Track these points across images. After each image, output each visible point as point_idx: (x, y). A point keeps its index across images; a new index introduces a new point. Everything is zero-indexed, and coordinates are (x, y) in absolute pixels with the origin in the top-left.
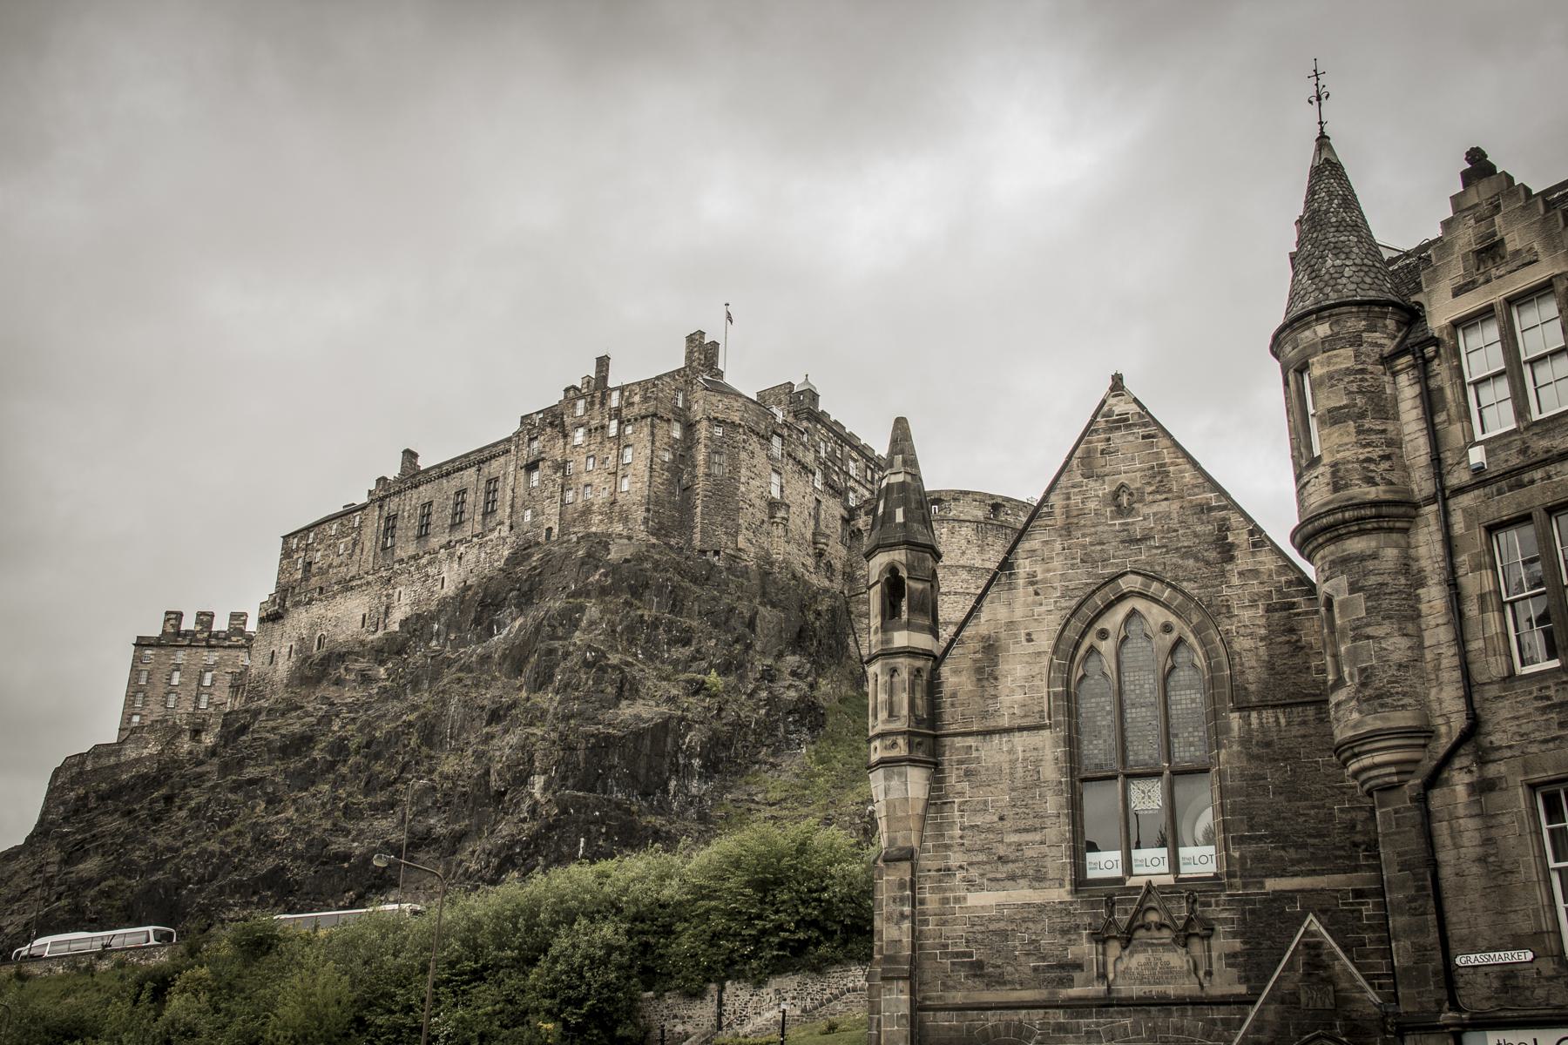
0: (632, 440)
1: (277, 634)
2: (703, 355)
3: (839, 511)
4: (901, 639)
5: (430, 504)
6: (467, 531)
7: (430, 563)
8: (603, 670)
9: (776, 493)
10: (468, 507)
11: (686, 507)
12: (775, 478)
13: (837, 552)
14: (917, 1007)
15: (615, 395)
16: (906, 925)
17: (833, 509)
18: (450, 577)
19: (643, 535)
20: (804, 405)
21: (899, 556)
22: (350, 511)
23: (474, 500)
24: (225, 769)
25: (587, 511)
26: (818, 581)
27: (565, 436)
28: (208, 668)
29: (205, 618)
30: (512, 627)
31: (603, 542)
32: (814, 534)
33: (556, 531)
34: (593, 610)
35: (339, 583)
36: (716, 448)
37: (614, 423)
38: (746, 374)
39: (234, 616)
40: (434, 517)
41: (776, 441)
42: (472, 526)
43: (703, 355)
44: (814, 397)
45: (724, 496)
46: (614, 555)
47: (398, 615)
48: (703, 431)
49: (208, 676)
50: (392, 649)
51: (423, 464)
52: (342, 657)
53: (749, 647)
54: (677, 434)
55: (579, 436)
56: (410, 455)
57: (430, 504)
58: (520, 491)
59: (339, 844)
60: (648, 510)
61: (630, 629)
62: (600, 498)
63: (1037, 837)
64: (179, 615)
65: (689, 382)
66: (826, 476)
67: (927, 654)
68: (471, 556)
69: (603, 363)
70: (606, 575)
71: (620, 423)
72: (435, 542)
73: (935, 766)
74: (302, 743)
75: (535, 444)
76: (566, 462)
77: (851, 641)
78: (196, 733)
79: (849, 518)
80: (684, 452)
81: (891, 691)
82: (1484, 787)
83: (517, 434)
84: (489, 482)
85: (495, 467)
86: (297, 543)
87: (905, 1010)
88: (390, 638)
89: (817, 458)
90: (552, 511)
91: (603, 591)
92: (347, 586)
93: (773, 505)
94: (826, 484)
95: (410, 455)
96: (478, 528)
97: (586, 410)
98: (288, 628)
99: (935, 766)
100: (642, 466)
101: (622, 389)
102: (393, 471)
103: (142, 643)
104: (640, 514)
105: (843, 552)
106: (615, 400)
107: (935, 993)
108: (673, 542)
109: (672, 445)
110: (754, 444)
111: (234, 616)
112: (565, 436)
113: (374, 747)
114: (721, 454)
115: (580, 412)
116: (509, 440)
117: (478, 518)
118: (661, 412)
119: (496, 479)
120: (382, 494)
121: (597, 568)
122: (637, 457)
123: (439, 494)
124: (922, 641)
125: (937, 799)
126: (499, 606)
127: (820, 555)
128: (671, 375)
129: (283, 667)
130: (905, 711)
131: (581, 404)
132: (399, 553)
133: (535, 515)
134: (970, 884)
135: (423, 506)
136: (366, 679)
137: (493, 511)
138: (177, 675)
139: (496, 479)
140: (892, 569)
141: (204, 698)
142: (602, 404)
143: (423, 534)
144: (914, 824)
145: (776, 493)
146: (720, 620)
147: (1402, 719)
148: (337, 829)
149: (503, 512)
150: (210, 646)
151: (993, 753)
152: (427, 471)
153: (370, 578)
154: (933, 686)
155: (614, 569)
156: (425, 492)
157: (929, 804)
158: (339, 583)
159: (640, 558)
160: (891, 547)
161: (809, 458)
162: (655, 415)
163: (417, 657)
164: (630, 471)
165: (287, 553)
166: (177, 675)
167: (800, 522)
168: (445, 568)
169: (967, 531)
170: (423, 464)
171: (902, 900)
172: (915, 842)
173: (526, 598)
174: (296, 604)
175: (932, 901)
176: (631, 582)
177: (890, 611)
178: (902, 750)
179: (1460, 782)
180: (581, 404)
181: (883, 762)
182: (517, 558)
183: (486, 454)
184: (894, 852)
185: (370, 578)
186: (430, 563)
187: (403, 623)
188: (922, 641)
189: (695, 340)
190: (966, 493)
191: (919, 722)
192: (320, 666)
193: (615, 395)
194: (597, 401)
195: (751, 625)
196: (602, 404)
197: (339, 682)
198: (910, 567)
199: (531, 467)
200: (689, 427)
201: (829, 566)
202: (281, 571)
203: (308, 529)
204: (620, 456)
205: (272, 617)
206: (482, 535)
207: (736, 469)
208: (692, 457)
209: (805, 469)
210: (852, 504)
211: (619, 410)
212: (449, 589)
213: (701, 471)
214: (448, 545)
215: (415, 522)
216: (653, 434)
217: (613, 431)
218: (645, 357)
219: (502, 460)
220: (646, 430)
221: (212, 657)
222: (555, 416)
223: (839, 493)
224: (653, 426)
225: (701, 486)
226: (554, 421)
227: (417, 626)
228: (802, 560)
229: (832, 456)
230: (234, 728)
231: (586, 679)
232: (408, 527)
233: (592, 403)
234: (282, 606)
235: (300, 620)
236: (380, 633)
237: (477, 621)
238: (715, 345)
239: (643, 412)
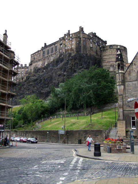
1: (31, 67)
3: (99, 48)
4: (120, 71)
6: (53, 53)
8: (72, 69)
9: (91, 46)
10: (53, 50)
11: (80, 49)
12: (91, 44)
13: (99, 53)
14: (123, 111)
15: (71, 35)
16: (122, 102)
17: (98, 47)
18: (52, 59)
20: (94, 35)
21: (120, 62)
22: (38, 51)
24: (27, 83)
25: (68, 50)
26: (97, 57)
32: (96, 51)
34: (70, 62)
36: (84, 41)
37: (71, 39)
38: (87, 31)
39: (25, 65)
41: (91, 40)
43: (82, 29)
44: (95, 34)
45: (85, 47)
47: (46, 63)
48: (82, 39)
52: (40, 69)
53: (89, 66)
56: (45, 44)
59: (42, 91)
61: (75, 64)
63: (136, 93)
65: (80, 33)
66: (97, 44)
67: (123, 73)
69: (69, 31)
72: (50, 54)
73: (124, 85)
74: (37, 80)
75: (61, 42)
76: (65, 44)
77: (101, 64)
78: (22, 79)
79: (100, 48)
80: (80, 42)
81: (119, 77)
83: (59, 41)
85: (56, 45)
86: (33, 55)
87: (122, 111)
88: (45, 66)
89: (96, 41)
90: (64, 50)
91: (71, 60)
92: (39, 60)
93: (91, 48)
94: (97, 45)
95: (45, 44)
96: (55, 53)
99: (124, 85)
101: (72, 34)
102: (43, 46)
105: (100, 53)
107: (125, 109)
109: (78, 41)
111: (25, 65)
113: (45, 80)
116: (58, 41)
122: (74, 42)
124: (123, 72)
125: (124, 89)
127: (97, 54)
128: (78, 32)
129: (32, 70)
130: (121, 79)
131: (67, 36)
134: (129, 98)
136: (43, 72)
140: (119, 64)
141: (23, 75)
144: (122, 91)
145: (91, 46)
146: (85, 63)
148: (42, 90)
149: (58, 50)
150: (23, 68)
151: (130, 83)
152: (48, 46)
154: (124, 77)
155: (72, 57)
156: (48, 48)
157: (124, 89)
159: (75, 55)
160: (118, 61)
161: (95, 42)
163: (49, 69)
164: (73, 44)
165: (31, 57)
167: (94, 50)
169: (115, 50)
171: (121, 100)
172: (122, 93)
175: (124, 100)
176: (75, 58)
177: (119, 68)
178: (121, 84)
180: (67, 36)
181: (119, 85)
182: (60, 56)
184: (120, 95)
187: (47, 65)
188: (123, 72)
190: (115, 45)
191: (122, 80)
192: (37, 70)
193: (71, 35)
195: (89, 63)
197: (39, 72)
198: (121, 63)
199: (61, 45)
200: (80, 39)
202: (31, 59)
203: (34, 54)
204: (72, 43)
205: (30, 65)
206: (55, 53)
208: (81, 42)
209: (95, 43)
210: (101, 47)
211: (71, 37)
212: (52, 60)
213: (82, 44)
214: (51, 55)
218: (75, 30)
220: (75, 39)
221: (23, 70)
222: (63, 38)
223: (99, 46)
225: (82, 46)
226: (63, 39)
227: (48, 65)
228: (95, 54)
230: (28, 78)
231: (70, 71)
232: (46, 53)
235: (34, 65)
238: (83, 28)
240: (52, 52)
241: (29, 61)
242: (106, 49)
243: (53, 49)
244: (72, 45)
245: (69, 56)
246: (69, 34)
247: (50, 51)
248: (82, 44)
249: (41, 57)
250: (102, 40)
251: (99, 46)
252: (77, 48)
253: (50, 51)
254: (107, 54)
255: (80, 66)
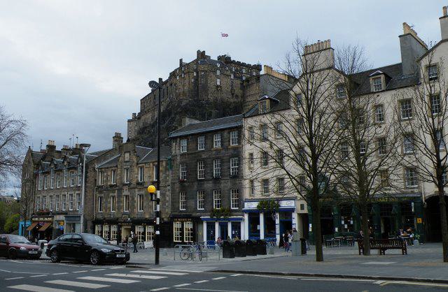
2: (201, 55)
9: (218, 84)
17: (239, 82)
31: (180, 101)
44: (230, 58)
45: (205, 88)
51: (164, 80)
54: (195, 75)
62: (181, 91)
93: (218, 86)
103: (129, 121)
110: (212, 74)
145: (218, 84)
159: (187, 104)
170: (164, 80)
189: (198, 52)
201: (237, 96)
218: (190, 57)
229: (236, 70)
242: (250, 83)
244: (185, 86)
250: (248, 66)
251: (241, 78)
254: (252, 93)
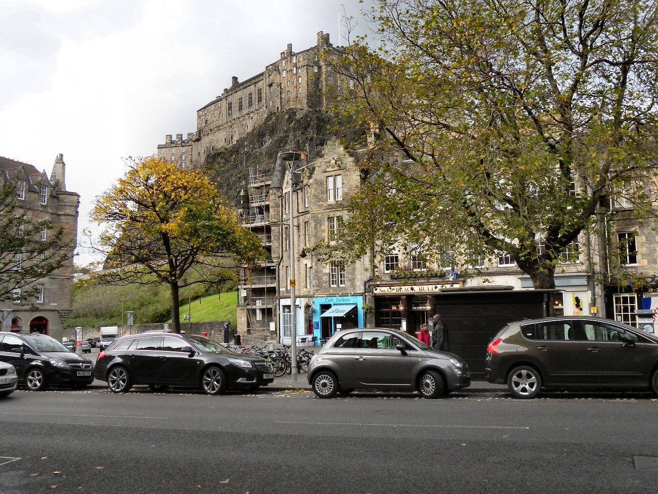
0: (301, 75)
1: (199, 146)
5: (241, 98)
7: (243, 120)
10: (253, 99)
11: (320, 97)
18: (250, 125)
19: (307, 108)
23: (255, 97)
27: (280, 74)
28: (183, 154)
29: (180, 136)
30: (268, 142)
33: (280, 108)
35: (216, 127)
40: (243, 103)
42: (255, 106)
43: (325, 39)
45: (332, 94)
46: (298, 116)
47: (236, 138)
48: (324, 69)
49: (184, 156)
50: (235, 150)
51: (240, 81)
52: (219, 154)
54: (316, 71)
55: (284, 74)
56: (235, 79)
57: (241, 98)
58: (268, 94)
60: (308, 99)
64: (171, 136)
68: (255, 117)
70: (295, 124)
71: (297, 68)
72: (245, 112)
75: (271, 77)
80: (318, 76)
82: (283, 266)
84: (259, 90)
85: (260, 85)
92: (219, 128)
93: (351, 92)
95: (235, 79)
97: (286, 64)
98: (202, 143)
100: (305, 84)
102: (229, 85)
104: (305, 101)
106: (294, 60)
108: (317, 109)
112: (280, 74)
114: (330, 76)
115: (284, 65)
117: (257, 103)
118: (310, 64)
119: (261, 89)
120: (226, 95)
121: (292, 121)
122: (303, 80)
123: (243, 94)
126: (264, 135)
129: (203, 158)
132: (235, 116)
133: (273, 103)
135: (239, 99)
137: (261, 100)
138: (173, 157)
139: (261, 89)
141: (183, 164)
142: (291, 62)
143: (241, 108)
147: (276, 256)
149: (264, 101)
153: (225, 126)
158: (216, 127)
159: (306, 116)
162: (307, 65)
164: (301, 86)
165: (199, 117)
166: (173, 157)
168: (248, 122)
170: (240, 81)
173: (272, 132)
174: (204, 135)
176: (304, 125)
179: (281, 264)
182: (268, 118)
183: (257, 80)
185: (225, 126)
186: (243, 120)
187: (237, 141)
194: (289, 60)
196: (291, 62)
199: (270, 85)
200: (320, 68)
202: (198, 123)
203: (205, 108)
207: (336, 82)
212: (249, 130)
214: (248, 114)
215: (237, 105)
216: (307, 72)
217: (295, 72)
218: (305, 41)
219: (262, 82)
220: (305, 71)
221: (184, 149)
222: (276, 67)
224: (307, 69)
226: (274, 68)
227: (241, 142)
232: (235, 107)
233: (287, 61)
234: (200, 136)
235: (205, 140)
236: (230, 145)
237: (258, 141)
239: (304, 65)
240: (250, 104)
241: (194, 130)
243: (253, 96)
245: (290, 119)
246: (289, 54)
247: (245, 103)
248: (324, 83)
249: (224, 117)
252: (310, 96)
253: (245, 103)
255: (317, 145)
